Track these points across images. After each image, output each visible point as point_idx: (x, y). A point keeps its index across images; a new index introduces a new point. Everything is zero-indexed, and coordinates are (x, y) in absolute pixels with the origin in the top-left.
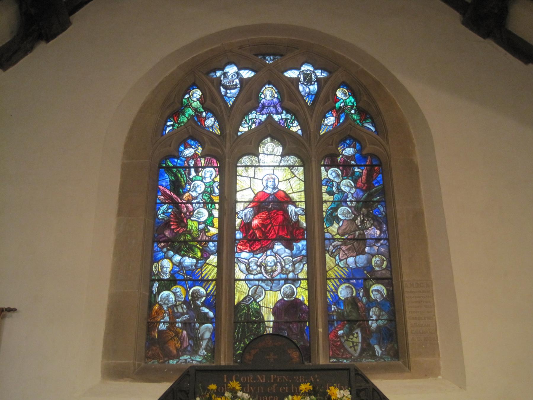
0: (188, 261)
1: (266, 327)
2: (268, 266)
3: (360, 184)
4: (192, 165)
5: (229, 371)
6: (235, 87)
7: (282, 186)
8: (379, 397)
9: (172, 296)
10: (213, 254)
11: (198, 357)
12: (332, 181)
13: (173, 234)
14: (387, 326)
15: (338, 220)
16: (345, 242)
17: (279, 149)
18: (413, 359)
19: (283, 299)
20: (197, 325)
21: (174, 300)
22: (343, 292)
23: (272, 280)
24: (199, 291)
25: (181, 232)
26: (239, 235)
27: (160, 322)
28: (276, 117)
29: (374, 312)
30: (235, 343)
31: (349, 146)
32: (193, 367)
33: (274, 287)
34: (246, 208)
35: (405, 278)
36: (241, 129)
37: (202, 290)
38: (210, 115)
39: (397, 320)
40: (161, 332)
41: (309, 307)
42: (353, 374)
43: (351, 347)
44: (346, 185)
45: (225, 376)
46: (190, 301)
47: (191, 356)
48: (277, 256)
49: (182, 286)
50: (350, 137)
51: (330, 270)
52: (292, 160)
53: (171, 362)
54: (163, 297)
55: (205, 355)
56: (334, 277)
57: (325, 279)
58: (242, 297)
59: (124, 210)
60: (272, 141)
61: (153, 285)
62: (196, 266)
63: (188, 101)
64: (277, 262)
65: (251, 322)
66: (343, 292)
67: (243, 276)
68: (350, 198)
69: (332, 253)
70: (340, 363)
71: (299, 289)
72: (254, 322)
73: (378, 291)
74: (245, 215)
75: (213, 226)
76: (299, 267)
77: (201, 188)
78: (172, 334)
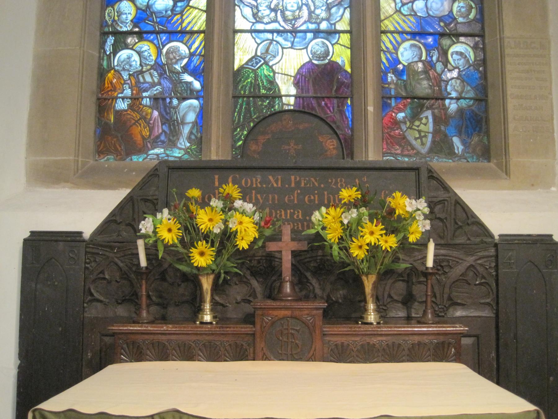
1: (283, 104)
2: (287, 10)
5: (222, 169)
8: (464, 215)
9: (136, 57)
11: (178, 151)
14: (473, 108)
18: (515, 160)
19: (310, 62)
20: (175, 102)
21: (138, 63)
22: (406, 53)
23: (294, 32)
24: (176, 50)
27: (117, 98)
33: (297, 43)
35: (507, 33)
37: (183, 49)
39: (490, 98)
40: (119, 114)
41: (351, 75)
42: (424, 175)
43: (416, 139)
45: (217, 177)
46: (165, 65)
47: (165, 149)
49: (151, 42)
51: (386, 18)
53: (135, 158)
54: (122, 59)
55: (188, 148)
56: (392, 29)
61: (106, 41)
62: (173, 10)
64: (302, 4)
65: (259, 97)
66: (406, 54)
67: (248, 26)
71: (336, 47)
73: (461, 54)
76: (336, 13)
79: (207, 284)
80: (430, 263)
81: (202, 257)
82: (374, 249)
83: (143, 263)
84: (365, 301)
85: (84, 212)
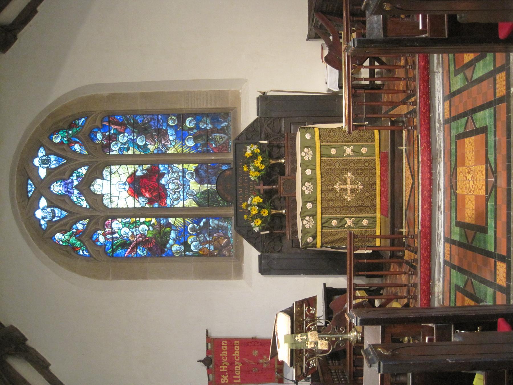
3: (122, 130)
4: (111, 236)
6: (53, 211)
7: (124, 178)
9: (194, 243)
10: (168, 221)
12: (120, 148)
13: (156, 246)
15: (146, 144)
16: (160, 141)
17: (99, 181)
18: (230, 105)
20: (211, 228)
22: (191, 143)
23: (183, 185)
24: (191, 229)
25: (154, 241)
27: (209, 250)
28: (76, 183)
29: (202, 126)
30: (221, 206)
31: (96, 136)
32: (235, 229)
34: (139, 202)
35: (183, 107)
36: (84, 206)
38: (74, 227)
40: (215, 249)
41: (199, 164)
42: (237, 141)
44: (123, 139)
48: (169, 182)
49: (188, 238)
50: (89, 135)
51: (177, 151)
52: (106, 173)
53: (232, 242)
57: (182, 154)
58: (194, 202)
60: (93, 186)
62: (175, 231)
63: (64, 242)
67: (181, 203)
68: (131, 137)
69: (167, 149)
70: (232, 146)
72: (208, 195)
73: (190, 123)
74: (143, 202)
75: (150, 221)
77: (126, 230)
78: (216, 242)
79: (273, 212)
80: (266, 142)
81: (265, 213)
82: (262, 162)
83: (268, 232)
84: (278, 163)
85: (251, 255)
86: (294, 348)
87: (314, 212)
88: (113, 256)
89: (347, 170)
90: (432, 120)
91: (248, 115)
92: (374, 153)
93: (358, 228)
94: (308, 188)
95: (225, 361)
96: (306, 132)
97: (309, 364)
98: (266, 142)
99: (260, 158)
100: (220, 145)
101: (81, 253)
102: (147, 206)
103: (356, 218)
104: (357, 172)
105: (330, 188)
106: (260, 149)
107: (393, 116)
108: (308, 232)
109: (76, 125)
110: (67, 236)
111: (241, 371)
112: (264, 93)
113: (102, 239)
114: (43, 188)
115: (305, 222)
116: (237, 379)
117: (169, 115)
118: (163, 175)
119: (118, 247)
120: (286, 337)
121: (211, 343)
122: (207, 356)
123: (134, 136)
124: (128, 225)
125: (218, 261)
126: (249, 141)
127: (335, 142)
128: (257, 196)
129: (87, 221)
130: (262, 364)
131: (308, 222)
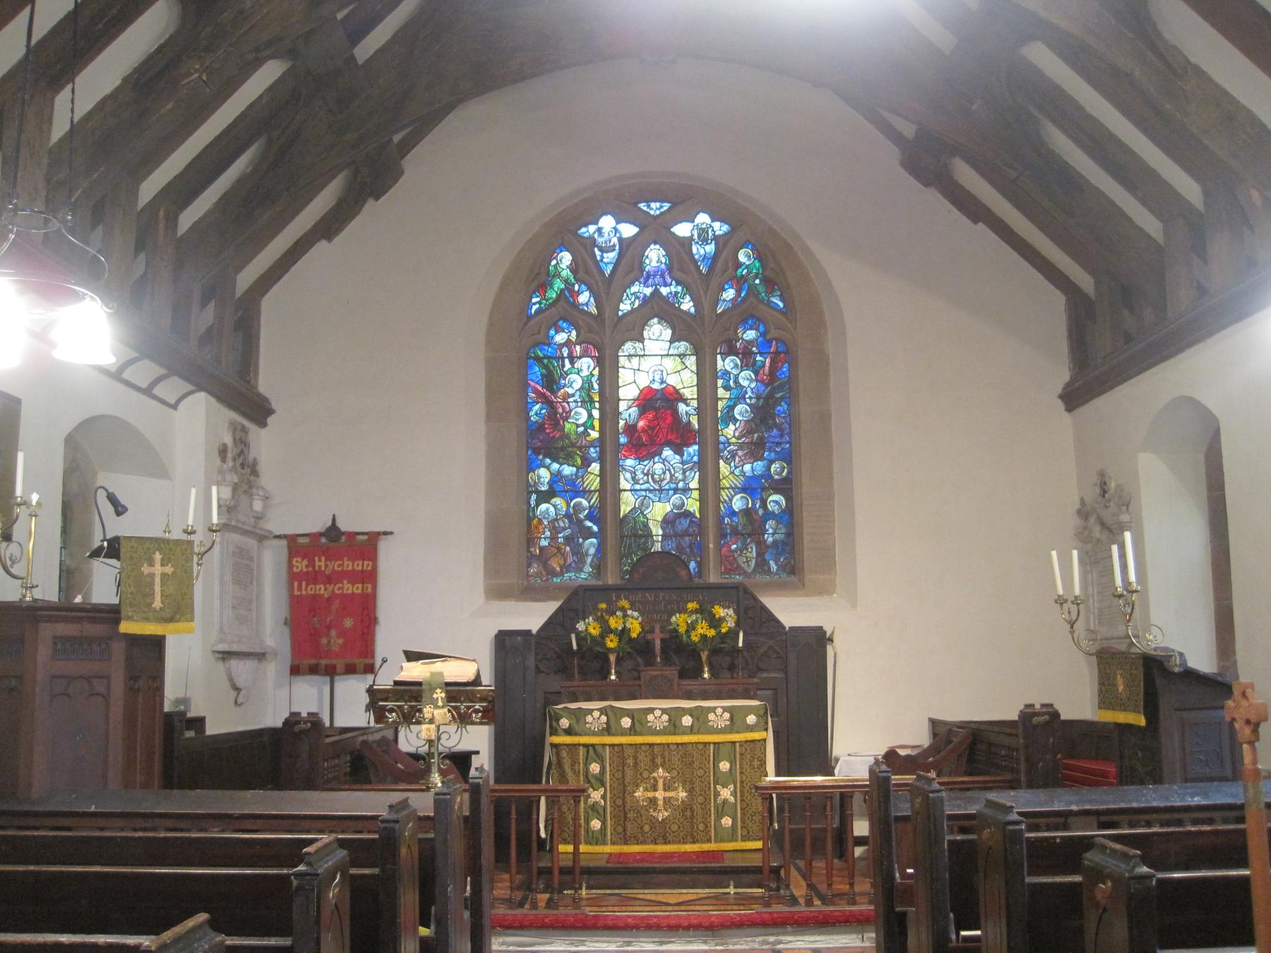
0: (568, 470)
5: (617, 589)
6: (612, 249)
7: (672, 380)
9: (552, 509)
12: (730, 373)
13: (547, 440)
15: (737, 420)
16: (741, 447)
17: (668, 333)
18: (809, 576)
23: (661, 490)
24: (580, 503)
26: (623, 440)
28: (664, 291)
29: (770, 525)
31: (751, 329)
32: (581, 586)
35: (805, 490)
36: (622, 307)
37: (585, 503)
40: (542, 549)
42: (741, 594)
44: (746, 378)
50: (752, 316)
52: (683, 346)
57: (718, 489)
59: (493, 415)
67: (628, 486)
68: (749, 394)
72: (642, 536)
73: (776, 502)
75: (593, 429)
77: (578, 384)
79: (612, 658)
80: (740, 644)
81: (612, 643)
82: (704, 637)
83: (575, 647)
85: (532, 617)
86: (424, 687)
87: (613, 731)
88: (527, 359)
89: (690, 791)
90: (780, 930)
91: (791, 611)
92: (722, 840)
93: (586, 811)
94: (657, 720)
95: (335, 566)
96: (758, 716)
97: (391, 711)
98: (740, 644)
99: (712, 633)
100: (735, 559)
101: (534, 300)
102: (622, 423)
103: (605, 809)
104: (687, 807)
105: (659, 760)
106: (727, 632)
107: (788, 873)
108: (578, 721)
109: (770, 291)
110: (566, 273)
111: (315, 597)
112: (831, 640)
113: (561, 338)
114: (655, 230)
115: (596, 714)
116: (300, 589)
117: (789, 462)
118: (678, 451)
119: (546, 367)
120: (441, 674)
121: (369, 539)
122: (343, 533)
123: (750, 398)
124: (587, 387)
125: (517, 554)
126: (742, 611)
127: (741, 768)
128: (642, 627)
129: (594, 310)
130: (328, 635)
131: (596, 720)
